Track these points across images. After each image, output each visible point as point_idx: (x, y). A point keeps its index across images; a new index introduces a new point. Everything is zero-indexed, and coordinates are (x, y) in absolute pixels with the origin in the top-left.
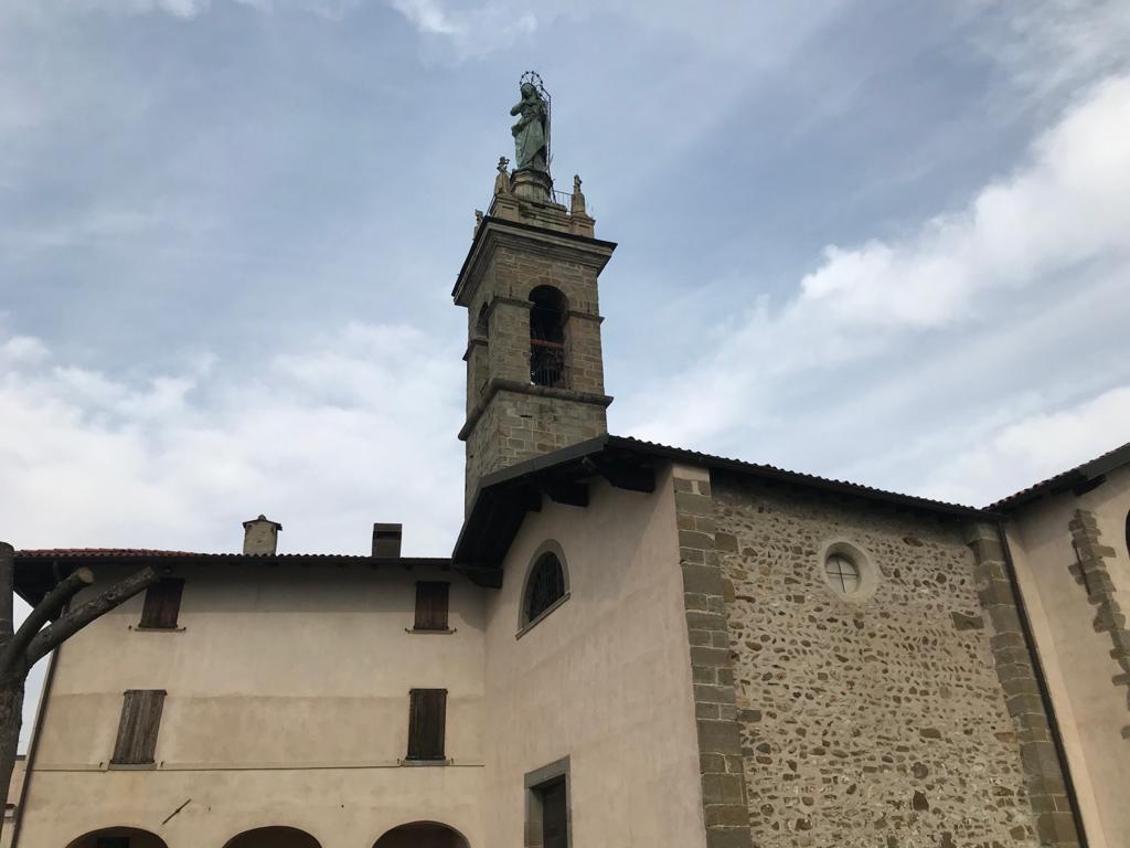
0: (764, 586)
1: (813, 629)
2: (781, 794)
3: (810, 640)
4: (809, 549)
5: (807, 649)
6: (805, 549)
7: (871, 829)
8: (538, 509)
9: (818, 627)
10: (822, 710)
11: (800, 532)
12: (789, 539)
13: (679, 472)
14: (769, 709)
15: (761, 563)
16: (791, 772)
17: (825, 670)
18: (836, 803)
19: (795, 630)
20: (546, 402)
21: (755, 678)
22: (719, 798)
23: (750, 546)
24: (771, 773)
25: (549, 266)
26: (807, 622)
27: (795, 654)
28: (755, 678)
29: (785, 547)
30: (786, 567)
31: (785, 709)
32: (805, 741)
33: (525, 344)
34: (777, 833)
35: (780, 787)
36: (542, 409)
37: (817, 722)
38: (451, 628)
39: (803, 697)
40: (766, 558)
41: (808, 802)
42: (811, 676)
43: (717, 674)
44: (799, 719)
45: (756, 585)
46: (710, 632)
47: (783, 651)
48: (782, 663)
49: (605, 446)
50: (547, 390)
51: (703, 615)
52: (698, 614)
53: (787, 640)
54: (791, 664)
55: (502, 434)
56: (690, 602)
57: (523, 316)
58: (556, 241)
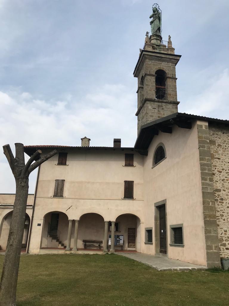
8: (157, 134)
13: (199, 123)
14: (223, 189)
15: (223, 148)
20: (160, 104)
21: (220, 180)
22: (208, 212)
23: (220, 144)
24: (223, 206)
25: (161, 64)
33: (154, 87)
34: (224, 222)
35: (226, 210)
36: (159, 106)
38: (134, 166)
40: (224, 147)
43: (208, 179)
45: (221, 155)
49: (177, 116)
50: (160, 100)
56: (201, 159)
57: (153, 79)
58: (163, 56)
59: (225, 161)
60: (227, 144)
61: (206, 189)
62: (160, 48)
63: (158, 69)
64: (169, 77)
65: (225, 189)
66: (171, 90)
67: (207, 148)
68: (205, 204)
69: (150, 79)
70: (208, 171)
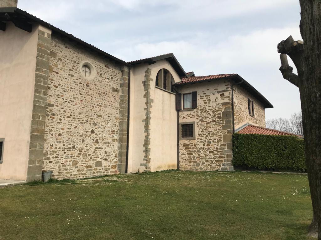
0: (62, 70)
1: (74, 84)
2: (55, 127)
3: (73, 87)
4: (78, 62)
5: (71, 90)
6: (77, 62)
7: (78, 137)
9: (76, 84)
10: (72, 107)
11: (76, 57)
12: (73, 58)
13: (41, 28)
15: (63, 63)
16: (60, 121)
17: (75, 96)
18: (71, 130)
19: (69, 84)
21: (54, 95)
22: (36, 126)
24: (54, 121)
26: (73, 82)
27: (67, 90)
28: (54, 95)
29: (71, 60)
30: (70, 66)
31: (62, 105)
32: (65, 114)
34: (52, 136)
35: (55, 125)
37: (70, 110)
39: (67, 102)
40: (65, 62)
41: (63, 129)
42: (71, 97)
43: (42, 93)
44: (65, 108)
46: (43, 80)
47: (64, 89)
48: (63, 92)
51: (41, 75)
52: (39, 74)
53: (66, 86)
54: (66, 93)
56: (37, 70)
61: (39, 102)
70: (44, 84)
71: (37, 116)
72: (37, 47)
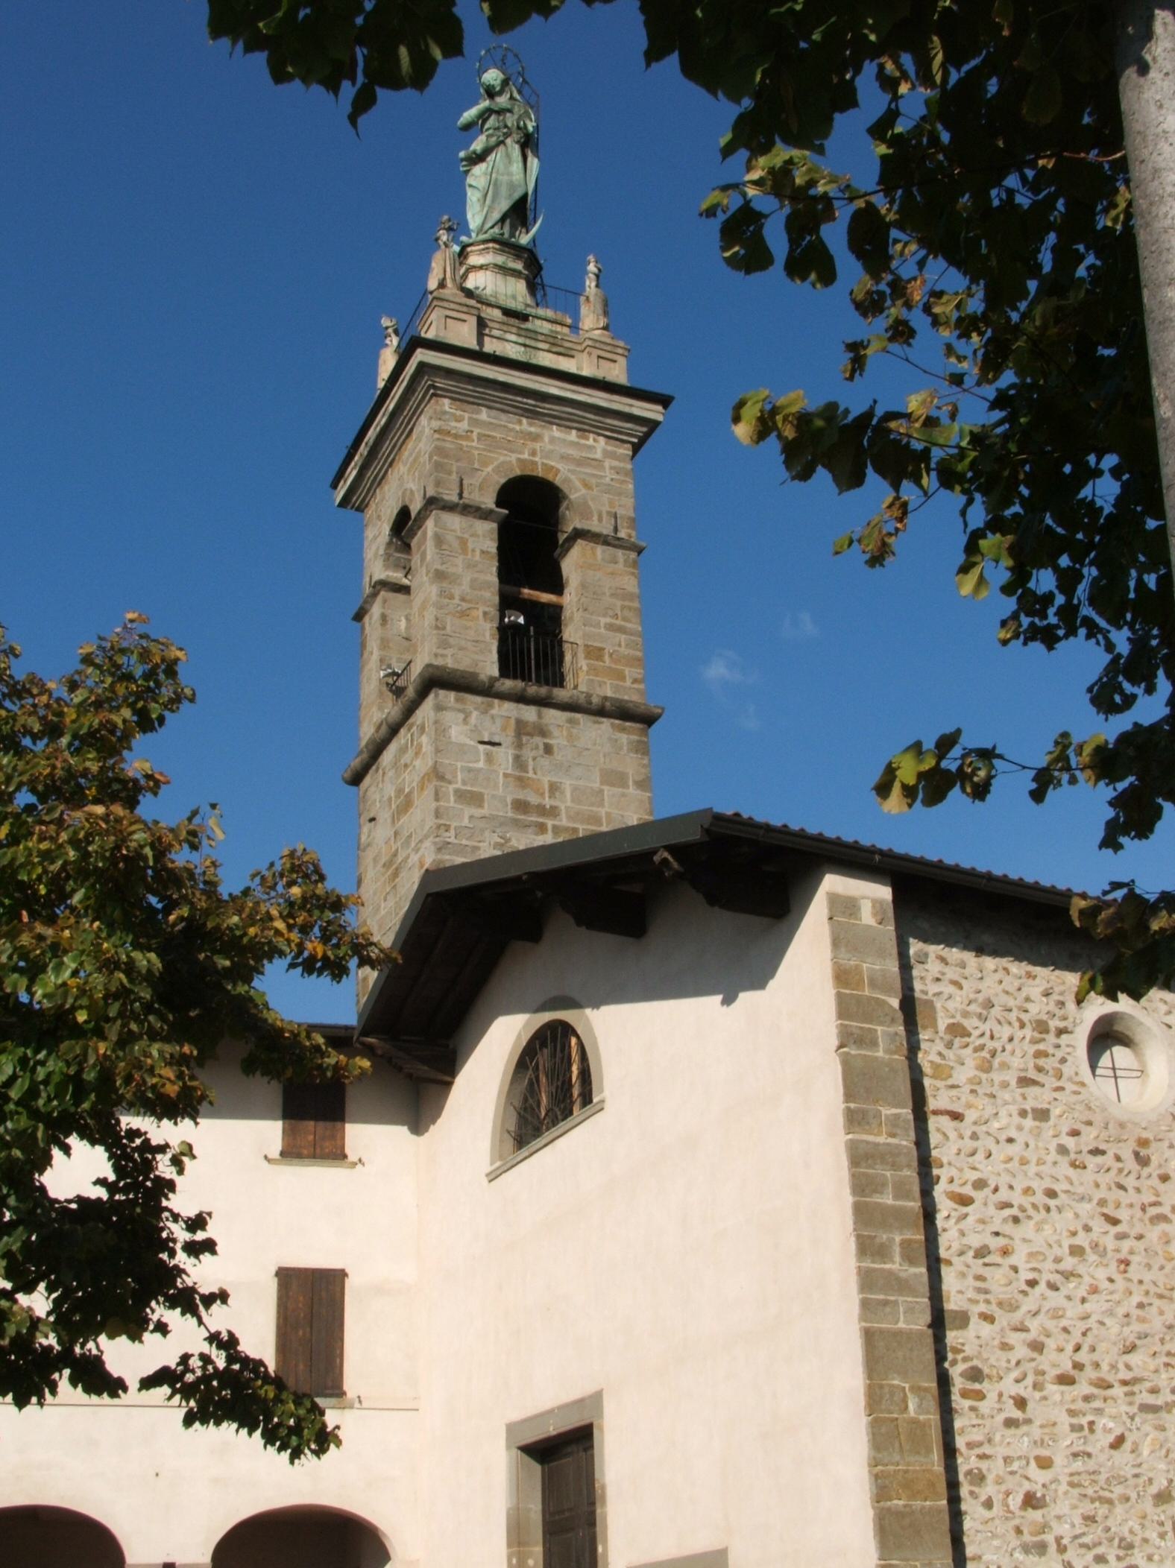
0: (980, 1091)
1: (1064, 1169)
2: (1000, 1451)
3: (1057, 1187)
4: (1062, 1024)
5: (1052, 1203)
6: (1054, 1024)
7: (1148, 1505)
8: (534, 934)
9: (1073, 1165)
10: (1073, 1310)
11: (1047, 994)
12: (1028, 1006)
13: (833, 883)
14: (982, 1307)
15: (976, 1050)
16: (1017, 1414)
17: (1082, 1240)
18: (1091, 1465)
19: (1032, 1169)
20: (529, 713)
21: (961, 1253)
22: (897, 1457)
23: (958, 1019)
24: (983, 1417)
25: (536, 438)
26: (1053, 1155)
27: (1031, 1211)
28: (961, 1253)
29: (1019, 1020)
30: (1019, 1059)
31: (1011, 1307)
32: (1044, 1361)
33: (487, 594)
34: (988, 1514)
35: (997, 1438)
36: (522, 729)
37: (1065, 1330)
38: (352, 1157)
39: (1042, 1287)
40: (986, 1040)
41: (1045, 1463)
42: (1057, 1251)
43: (897, 1249)
44: (1034, 1325)
45: (967, 1088)
46: (888, 1174)
47: (1012, 1206)
48: (1008, 1228)
49: (707, 831)
50: (533, 690)
51: (878, 1144)
52: (867, 1142)
53: (1019, 1188)
54: (1027, 1229)
55: (441, 778)
56: (854, 1119)
57: (484, 538)
58: (553, 388)
59: (988, 1133)
60: (1000, 1023)
61: (888, 1309)
62: (533, 334)
63: (518, 472)
64: (589, 531)
65: (994, 1309)
66: (603, 621)
67: (886, 1051)
68: (882, 1412)
69: (458, 538)
70: (896, 1197)
71: (892, 1394)
72: (834, 992)
